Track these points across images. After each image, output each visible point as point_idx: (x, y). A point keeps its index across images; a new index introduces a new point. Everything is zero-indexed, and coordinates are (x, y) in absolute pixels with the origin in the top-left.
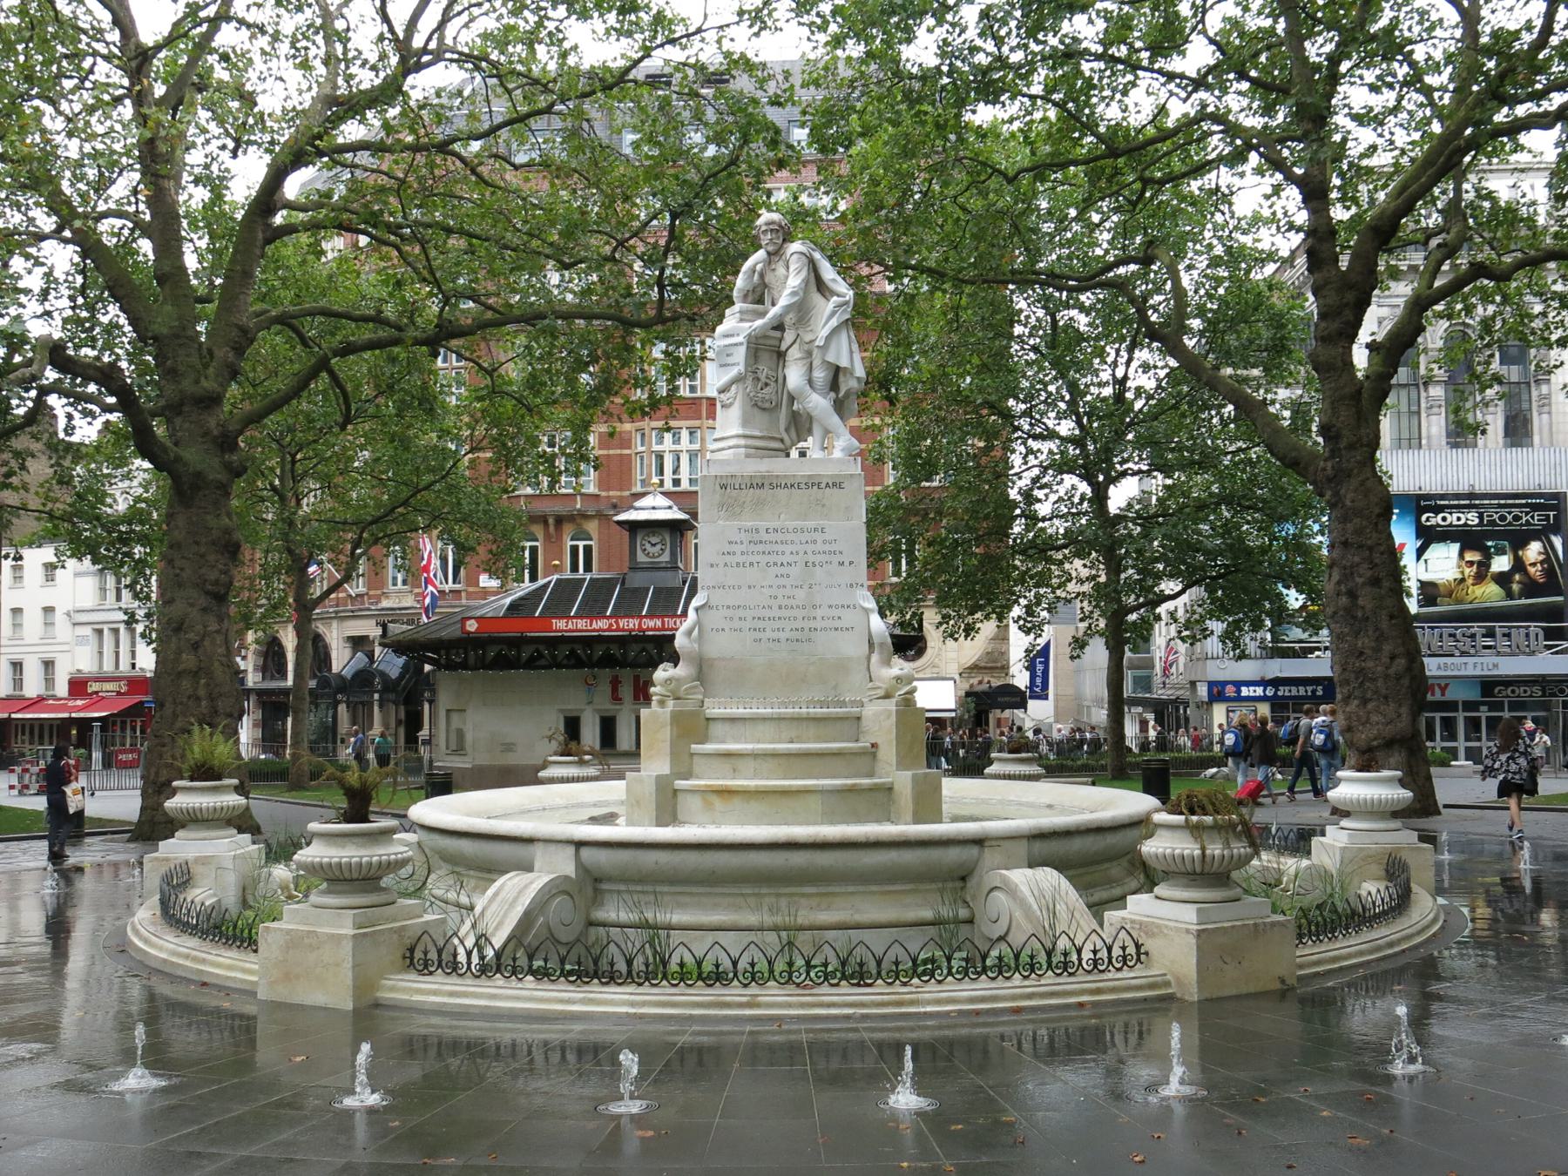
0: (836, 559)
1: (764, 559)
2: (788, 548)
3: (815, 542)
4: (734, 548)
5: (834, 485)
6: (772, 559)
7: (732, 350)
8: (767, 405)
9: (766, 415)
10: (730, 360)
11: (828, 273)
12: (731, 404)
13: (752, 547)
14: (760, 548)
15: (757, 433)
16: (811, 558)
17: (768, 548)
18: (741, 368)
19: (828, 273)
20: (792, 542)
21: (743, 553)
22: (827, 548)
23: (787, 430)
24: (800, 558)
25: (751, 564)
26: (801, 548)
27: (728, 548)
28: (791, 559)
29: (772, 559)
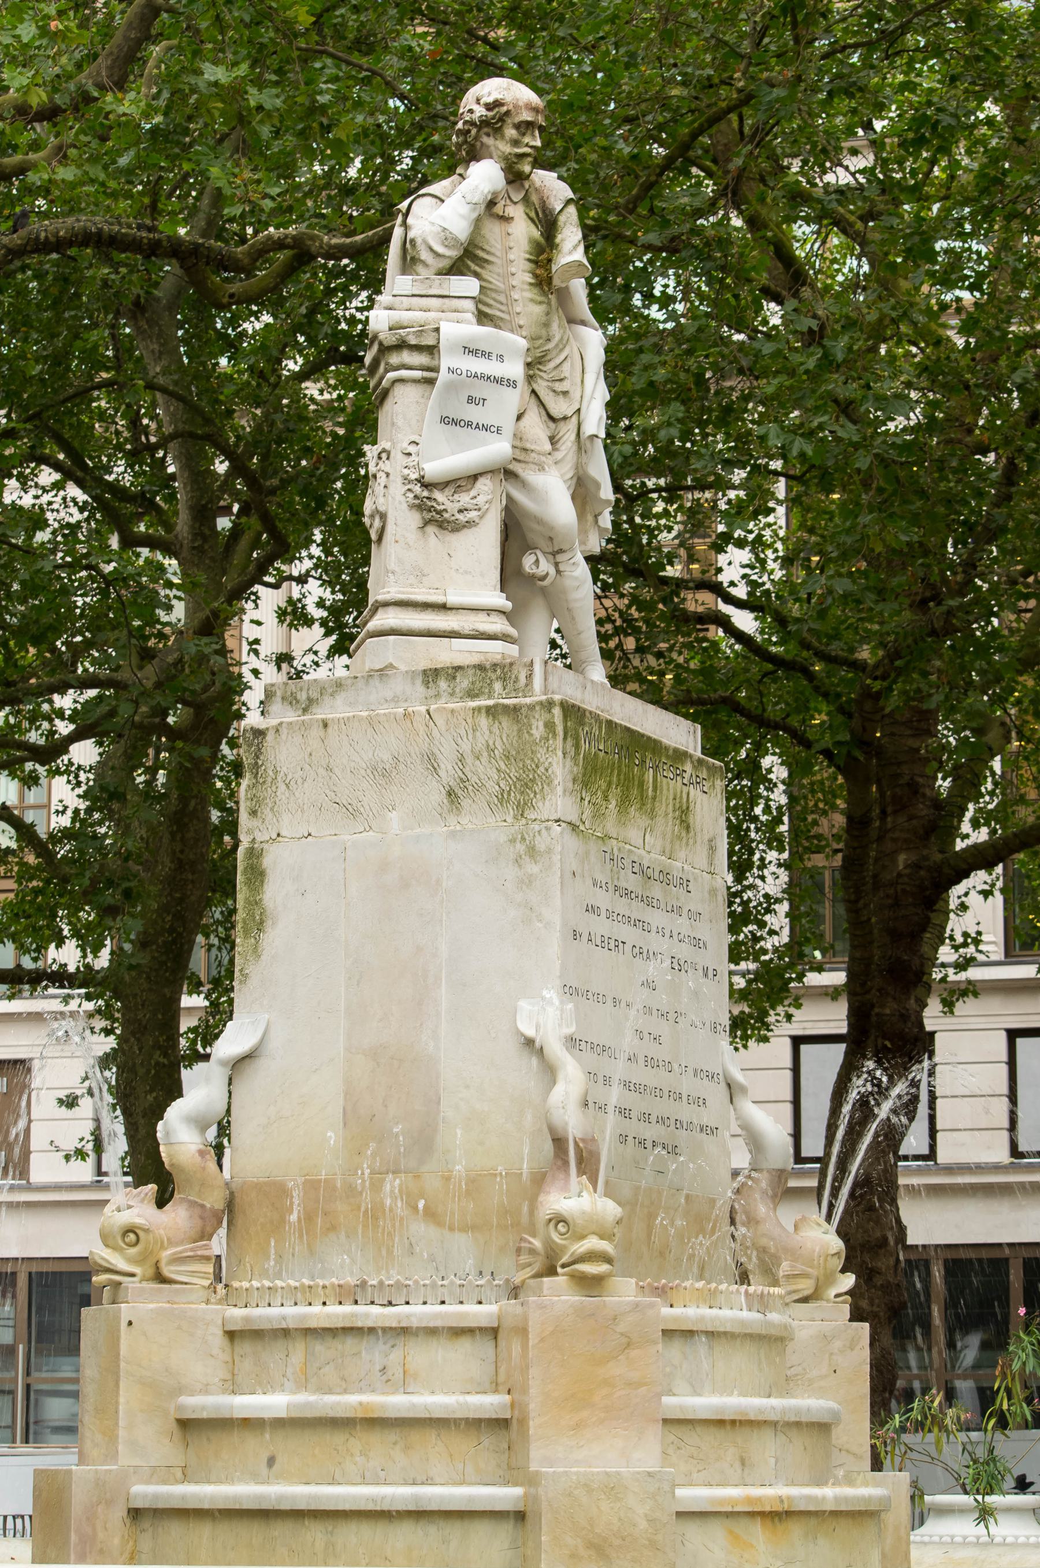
10: (474, 413)
12: (469, 524)
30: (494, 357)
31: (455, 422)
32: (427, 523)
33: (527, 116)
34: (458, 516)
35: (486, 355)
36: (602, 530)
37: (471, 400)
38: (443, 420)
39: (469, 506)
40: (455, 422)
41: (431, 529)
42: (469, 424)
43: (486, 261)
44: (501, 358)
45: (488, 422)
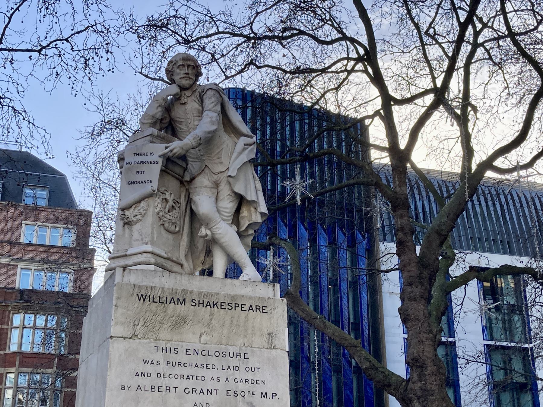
0: (259, 389)
1: (183, 384)
2: (208, 374)
3: (237, 368)
4: (148, 368)
5: (257, 308)
6: (191, 384)
7: (144, 167)
8: (172, 228)
9: (171, 237)
10: (140, 178)
11: (236, 117)
13: (170, 370)
14: (178, 370)
15: (163, 254)
16: (232, 386)
17: (186, 371)
18: (155, 185)
19: (236, 117)
20: (214, 367)
21: (159, 375)
22: (250, 376)
23: (186, 256)
24: (221, 386)
25: (168, 389)
26: (223, 375)
27: (142, 368)
28: (211, 385)
29: (191, 384)
30: (149, 154)
31: (132, 183)
32: (125, 224)
33: (181, 63)
34: (133, 219)
35: (146, 154)
36: (262, 214)
37: (138, 173)
38: (128, 183)
39: (137, 214)
40: (132, 183)
41: (126, 226)
42: (139, 182)
43: (182, 122)
44: (152, 154)
45: (146, 179)
